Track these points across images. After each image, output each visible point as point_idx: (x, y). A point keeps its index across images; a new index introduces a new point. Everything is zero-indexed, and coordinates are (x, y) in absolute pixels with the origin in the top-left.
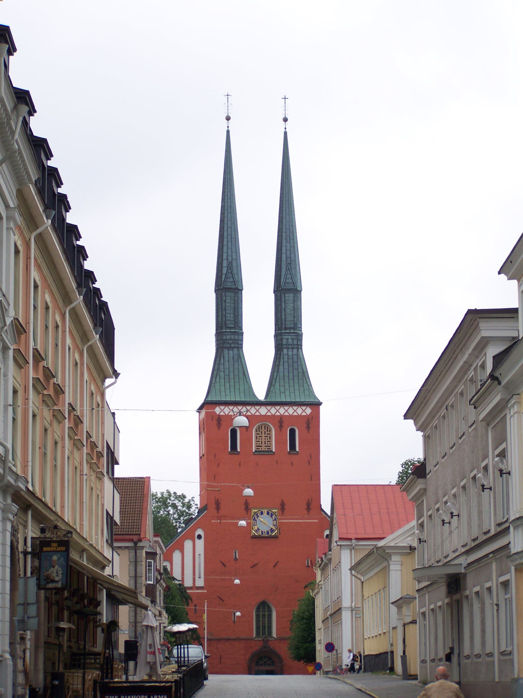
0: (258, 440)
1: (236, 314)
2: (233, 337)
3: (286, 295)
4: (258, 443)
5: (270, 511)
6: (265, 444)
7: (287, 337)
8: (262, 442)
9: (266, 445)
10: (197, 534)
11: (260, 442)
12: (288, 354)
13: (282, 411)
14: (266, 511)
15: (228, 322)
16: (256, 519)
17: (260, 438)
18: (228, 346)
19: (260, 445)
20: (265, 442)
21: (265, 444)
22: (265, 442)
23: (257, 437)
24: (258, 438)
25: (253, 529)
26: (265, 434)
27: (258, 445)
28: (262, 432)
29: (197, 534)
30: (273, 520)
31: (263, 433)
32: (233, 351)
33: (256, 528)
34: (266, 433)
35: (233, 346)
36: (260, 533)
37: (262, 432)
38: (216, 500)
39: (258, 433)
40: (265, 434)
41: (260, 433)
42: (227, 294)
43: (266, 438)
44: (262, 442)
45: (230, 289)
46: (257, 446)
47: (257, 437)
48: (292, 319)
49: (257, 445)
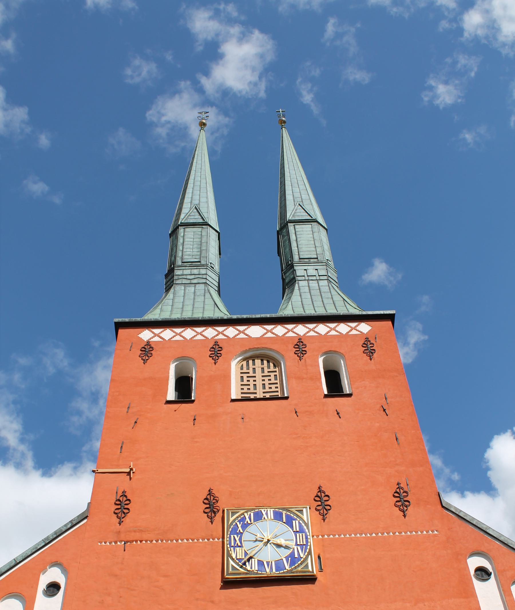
0: (245, 382)
1: (204, 248)
2: (196, 271)
3: (297, 227)
4: (245, 388)
5: (284, 509)
6: (264, 388)
7: (306, 268)
8: (255, 385)
9: (267, 390)
10: (44, 581)
11: (252, 387)
12: (309, 286)
13: (301, 330)
14: (271, 512)
15: (185, 257)
16: (240, 528)
17: (251, 379)
18: (185, 281)
19: (252, 390)
20: (264, 384)
21: (264, 388)
22: (264, 384)
23: (242, 377)
24: (245, 379)
25: (229, 555)
26: (263, 371)
27: (245, 390)
28: (254, 369)
29: (44, 581)
30: (296, 532)
31: (258, 371)
32: (195, 287)
33: (239, 553)
34: (266, 370)
35: (195, 281)
36: (255, 567)
37: (254, 369)
38: (120, 493)
39: (245, 370)
40: (263, 371)
41: (251, 371)
42: (187, 230)
43: (266, 379)
44: (255, 385)
45: (194, 225)
46: (242, 393)
47: (242, 377)
48: (314, 249)
49: (243, 391)
